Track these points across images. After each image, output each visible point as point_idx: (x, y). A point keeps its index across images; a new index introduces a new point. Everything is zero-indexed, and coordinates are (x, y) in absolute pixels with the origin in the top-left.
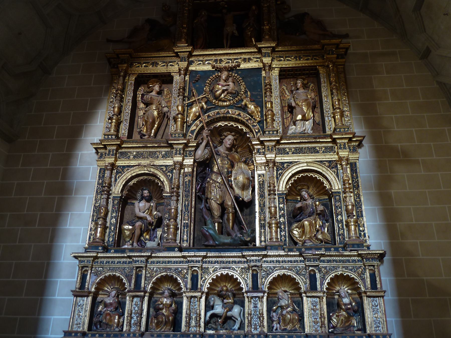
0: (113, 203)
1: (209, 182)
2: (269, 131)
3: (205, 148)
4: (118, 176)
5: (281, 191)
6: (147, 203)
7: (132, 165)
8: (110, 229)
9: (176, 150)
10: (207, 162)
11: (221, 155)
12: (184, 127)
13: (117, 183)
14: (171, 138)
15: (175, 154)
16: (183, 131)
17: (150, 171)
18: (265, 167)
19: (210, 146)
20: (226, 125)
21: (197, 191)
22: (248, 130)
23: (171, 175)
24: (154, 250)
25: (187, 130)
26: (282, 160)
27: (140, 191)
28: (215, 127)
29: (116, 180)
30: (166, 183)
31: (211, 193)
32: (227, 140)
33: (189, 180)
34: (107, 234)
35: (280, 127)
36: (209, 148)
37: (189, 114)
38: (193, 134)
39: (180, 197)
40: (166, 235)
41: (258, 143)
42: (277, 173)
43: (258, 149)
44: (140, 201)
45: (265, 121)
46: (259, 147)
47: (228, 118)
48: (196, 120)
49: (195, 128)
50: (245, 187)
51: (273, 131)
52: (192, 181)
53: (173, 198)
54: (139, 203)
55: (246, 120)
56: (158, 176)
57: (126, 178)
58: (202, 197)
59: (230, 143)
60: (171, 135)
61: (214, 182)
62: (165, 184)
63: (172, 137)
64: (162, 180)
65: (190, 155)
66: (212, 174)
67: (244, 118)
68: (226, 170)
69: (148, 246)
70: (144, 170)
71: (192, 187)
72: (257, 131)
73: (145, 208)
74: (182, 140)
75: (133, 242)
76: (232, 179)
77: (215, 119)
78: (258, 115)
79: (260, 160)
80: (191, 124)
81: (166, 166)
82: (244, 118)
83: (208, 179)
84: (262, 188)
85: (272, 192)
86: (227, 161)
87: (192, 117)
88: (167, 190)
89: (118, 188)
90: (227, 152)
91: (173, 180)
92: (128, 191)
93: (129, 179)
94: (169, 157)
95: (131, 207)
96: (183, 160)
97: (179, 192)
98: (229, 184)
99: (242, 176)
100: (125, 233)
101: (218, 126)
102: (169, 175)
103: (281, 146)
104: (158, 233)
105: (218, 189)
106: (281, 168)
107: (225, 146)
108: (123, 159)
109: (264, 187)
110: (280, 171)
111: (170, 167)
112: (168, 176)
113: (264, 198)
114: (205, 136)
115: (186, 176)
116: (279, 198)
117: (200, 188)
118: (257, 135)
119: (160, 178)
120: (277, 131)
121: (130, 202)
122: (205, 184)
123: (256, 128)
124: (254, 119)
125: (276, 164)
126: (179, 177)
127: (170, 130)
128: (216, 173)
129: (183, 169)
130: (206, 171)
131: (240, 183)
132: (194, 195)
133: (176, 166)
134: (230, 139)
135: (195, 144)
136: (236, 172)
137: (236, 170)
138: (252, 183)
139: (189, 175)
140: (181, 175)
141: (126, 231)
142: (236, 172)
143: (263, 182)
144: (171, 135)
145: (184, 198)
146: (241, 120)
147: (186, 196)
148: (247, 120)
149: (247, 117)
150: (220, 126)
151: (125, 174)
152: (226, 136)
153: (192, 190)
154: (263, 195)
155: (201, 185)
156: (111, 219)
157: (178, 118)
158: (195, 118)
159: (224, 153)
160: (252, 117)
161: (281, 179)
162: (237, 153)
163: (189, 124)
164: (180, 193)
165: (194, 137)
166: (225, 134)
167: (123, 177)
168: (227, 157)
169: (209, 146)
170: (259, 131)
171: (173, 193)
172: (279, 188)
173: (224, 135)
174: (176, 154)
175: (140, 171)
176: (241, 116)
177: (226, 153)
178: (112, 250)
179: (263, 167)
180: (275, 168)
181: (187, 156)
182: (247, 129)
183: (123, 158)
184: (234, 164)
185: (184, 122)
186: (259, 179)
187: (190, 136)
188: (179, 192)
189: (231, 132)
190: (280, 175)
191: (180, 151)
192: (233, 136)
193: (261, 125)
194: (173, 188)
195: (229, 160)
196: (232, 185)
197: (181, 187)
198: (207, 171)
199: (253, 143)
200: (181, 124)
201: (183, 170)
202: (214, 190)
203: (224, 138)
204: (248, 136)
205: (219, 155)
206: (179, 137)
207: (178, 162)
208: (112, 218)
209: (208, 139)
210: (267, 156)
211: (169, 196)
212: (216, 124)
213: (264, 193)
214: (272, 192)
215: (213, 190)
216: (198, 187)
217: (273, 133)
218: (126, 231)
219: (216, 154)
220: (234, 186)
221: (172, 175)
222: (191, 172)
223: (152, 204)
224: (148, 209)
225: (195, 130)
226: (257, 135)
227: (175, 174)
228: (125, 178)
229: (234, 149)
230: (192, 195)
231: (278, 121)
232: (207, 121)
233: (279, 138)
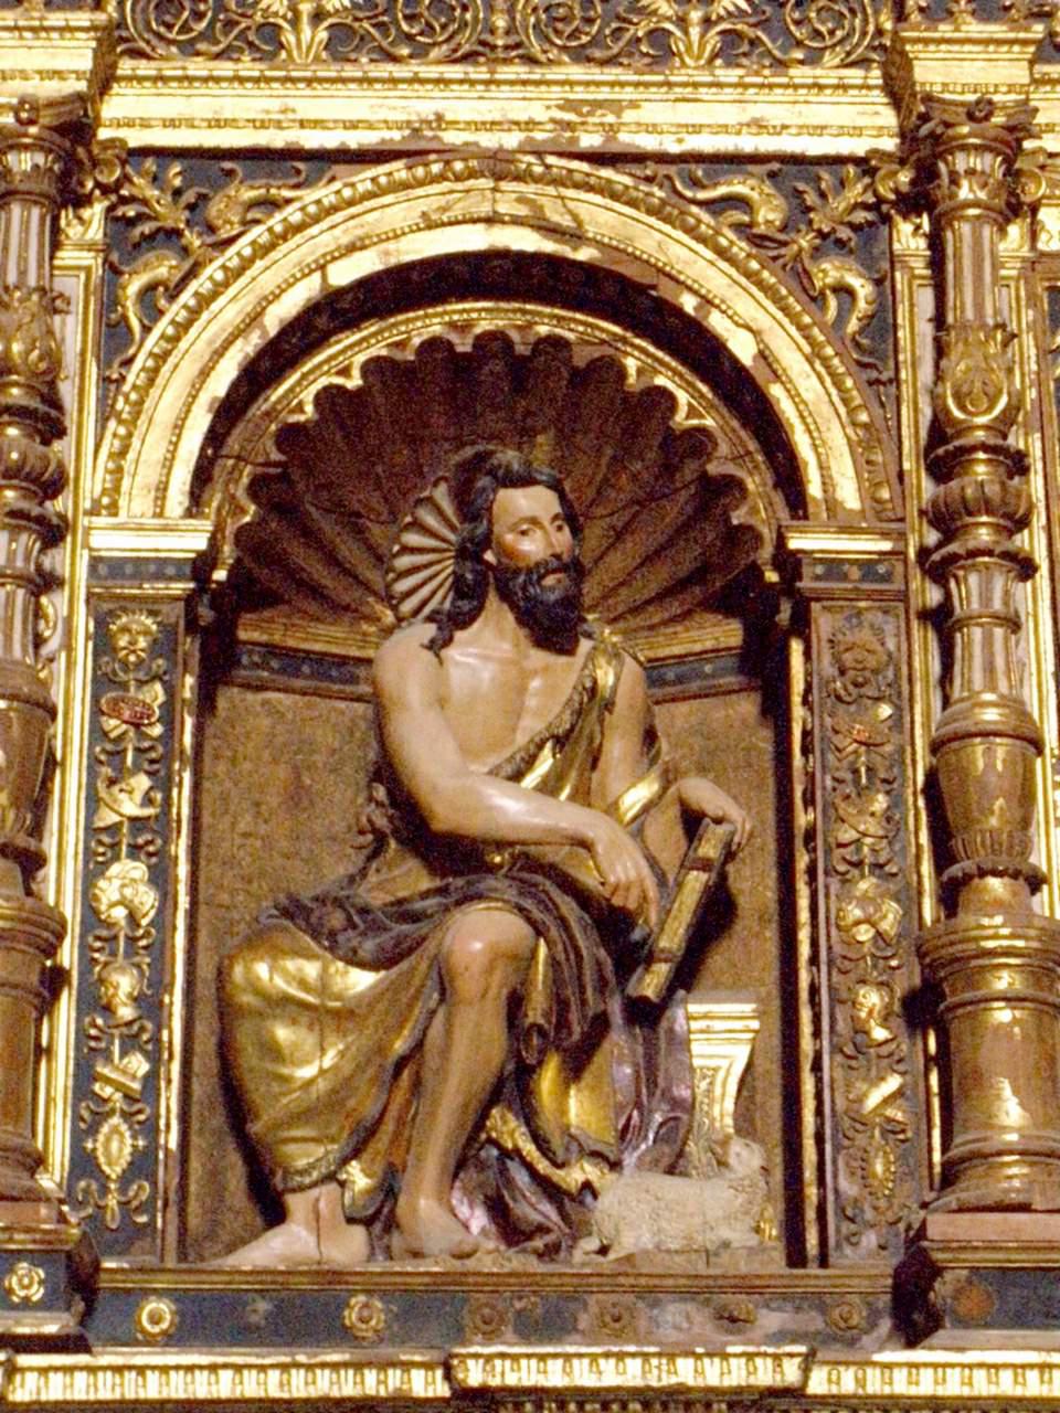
0: (103, 642)
4: (133, 286)
6: (539, 657)
7: (311, 140)
8: (94, 1002)
13: (134, 376)
17: (576, 237)
23: (863, 289)
24: (740, 1303)
27: (441, 494)
29: (114, 339)
30: (809, 384)
34: (59, 1074)
40: (893, 1083)
44: (452, 622)
54: (436, 646)
56: (689, 303)
57: (254, 318)
62: (787, 409)
64: (743, 348)
69: (629, 1241)
70: (491, 220)
73: (517, 713)
75: (388, 1189)
81: (788, 169)
88: (827, 483)
89: (150, 447)
92: (254, 489)
93: (288, 329)
94: (813, 59)
95: (271, 709)
100: (273, 1052)
102: (844, 291)
104: (703, 1052)
108: (197, 67)
119: (717, 322)
121: (272, 650)
141: (283, 1033)
151: (230, 256)
156: (93, 871)
167: (204, 301)
175: (430, 224)
178: (147, 1293)
183: (189, 49)
208: (102, 848)
211: (868, 567)
223: (606, 676)
224: (561, 741)
228: (228, 312)
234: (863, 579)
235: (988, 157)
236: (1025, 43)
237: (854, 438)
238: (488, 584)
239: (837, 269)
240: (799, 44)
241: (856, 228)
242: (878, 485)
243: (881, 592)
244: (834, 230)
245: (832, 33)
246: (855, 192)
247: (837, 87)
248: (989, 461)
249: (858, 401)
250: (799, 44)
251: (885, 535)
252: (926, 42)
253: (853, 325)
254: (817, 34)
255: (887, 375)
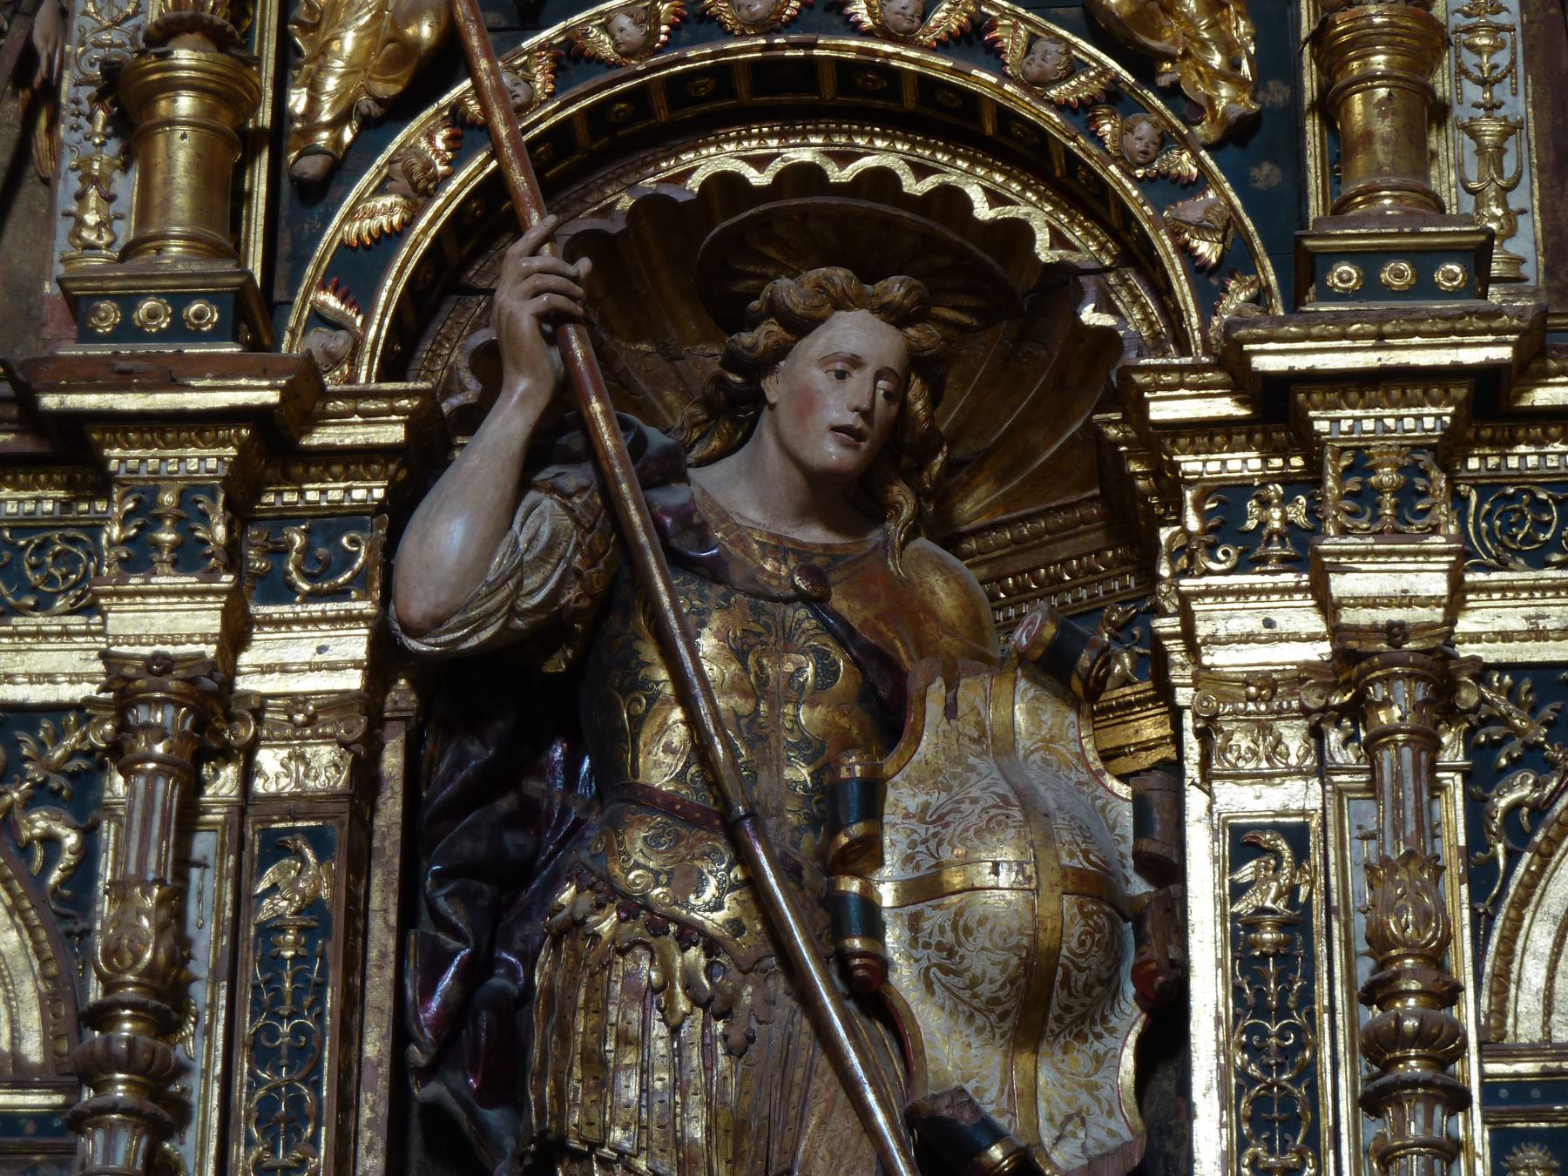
1: (575, 926)
2: (1368, 260)
3: (524, 484)
5: (1533, 1051)
9: (146, 514)
10: (557, 664)
11: (737, 576)
12: (241, 198)
14: (71, 351)
15: (129, 566)
16: (236, 252)
18: (1317, 734)
19: (591, 451)
20: (808, 176)
21: (418, 1056)
22: (1088, 247)
23: (71, 839)
25: (284, 247)
26: (1539, 635)
28: (650, 205)
31: (601, 1075)
32: (819, 378)
33: (312, 906)
35: (1517, 200)
36: (573, 478)
37: (306, 28)
38: (361, 298)
39: (191, 1135)
41: (1224, 407)
42: (1476, 809)
43: (1231, 495)
45: (1312, 126)
46: (1243, 463)
47: (828, 87)
48: (399, 110)
49: (387, 210)
50: (1059, 996)
51: (1426, 258)
52: (357, 911)
53: (92, 1146)
55: (1061, 107)
58: (483, 1128)
59: (851, 419)
60: (78, 305)
61: (637, 930)
63: (87, 335)
65: (328, 569)
66: (615, 826)
67: (1035, 85)
68: (803, 773)
71: (353, 1001)
72: (1207, 249)
74: (225, 371)
76: (887, 894)
77: (659, 101)
78: (1230, 50)
79: (1248, 638)
80: (342, 167)
82: (1035, 85)
83: (566, 895)
84: (1283, 1012)
85: (1413, 1067)
86: (821, 656)
87: (352, 70)
90: (815, 535)
91: (105, 907)
94: (43, 605)
96: (236, 635)
97: (182, 1070)
98: (839, 961)
99: (1007, 854)
101: (694, 183)
102: (51, 842)
103: (1524, 457)
105: (692, 1030)
106: (1533, 748)
107: (791, 455)
109: (1307, 996)
110: (1522, 790)
111: (57, 738)
112: (26, 850)
113: (1313, 1140)
114: (526, 323)
115: (276, 849)
116: (1503, 1143)
117: (457, 1016)
118: (1208, 309)
120: (1477, 256)
122: (530, 960)
123: (1192, 210)
124: (1172, 94)
125: (1468, 696)
126: (183, 862)
127: (61, 245)
128: (664, 804)
129: (225, 755)
130: (533, 786)
131: (981, 938)
132: (372, 1106)
133: (141, 715)
134: (855, 362)
135: (393, 433)
136: (937, 798)
137: (932, 776)
138: (1152, 951)
139: (317, 839)
140: (204, 844)
142: (937, 798)
143: (1296, 923)
144: (78, 305)
145: (238, 1151)
146: (1006, 116)
147: (265, 1114)
148: (1081, 113)
149: (1075, 67)
150: (727, 183)
152: (801, 326)
153: (350, 1035)
154: (1288, 1101)
155: (473, 975)
157: (172, 87)
158: (388, 89)
159: (779, 548)
160: (1144, 64)
161: (1530, 885)
162: (951, 540)
163: (312, 167)
164: (196, 1083)
165: (376, 330)
166: (790, 290)
168: (815, 602)
169: (571, 459)
170: (1236, 261)
171: (91, 1071)
172: (1500, 1010)
173: (775, 310)
174: (139, 556)
176: (993, 55)
177: (802, 552)
179: (1293, 738)
180: (1452, 750)
181: (285, 593)
182: (1075, 235)
184: (914, 685)
185: (248, 143)
186: (1238, 891)
187: (319, 318)
188: (182, 1070)
189: (870, 273)
190: (1518, 840)
191: (189, 516)
192: (897, 317)
193: (1266, 174)
194: (101, 1017)
195: (844, 635)
196: (881, 965)
197: (200, 994)
198: (547, 788)
199: (1161, 411)
200: (203, 165)
201: (230, 773)
202: (641, 1041)
203: (781, 352)
204: (1089, 316)
205: (713, 572)
206: (180, 331)
207: (162, 665)
209: (568, 357)
210: (1340, 585)
211: (42, 1119)
212: (669, 167)
213: (1309, 1073)
214: (1413, 1067)
215: (624, 1039)
216: (427, 991)
217: (1424, 287)
218: (102, 601)
219: (677, 561)
220: (904, 978)
221: (89, 834)
222: (333, 796)
225: (388, 240)
226: (1208, 309)
227: (124, 827)
229: (903, 497)
230: (347, 1103)
231: (1490, 129)
232: (545, 117)
233: (1505, 353)
234: (38, 1133)
235: (170, 711)
236: (216, 593)
237: (43, 988)
238: (1115, 993)
239: (45, 819)
240: (33, 590)
241: (73, 776)
242: (58, 1037)
243: (54, 1146)
244: (46, 779)
245: (65, 577)
246: (70, 742)
247: (59, 635)
248: (131, 1019)
249: (50, 954)
250: (33, 590)
251: (58, 1089)
252: (120, 595)
253: (55, 877)
254: (50, 580)
255: (82, 925)
